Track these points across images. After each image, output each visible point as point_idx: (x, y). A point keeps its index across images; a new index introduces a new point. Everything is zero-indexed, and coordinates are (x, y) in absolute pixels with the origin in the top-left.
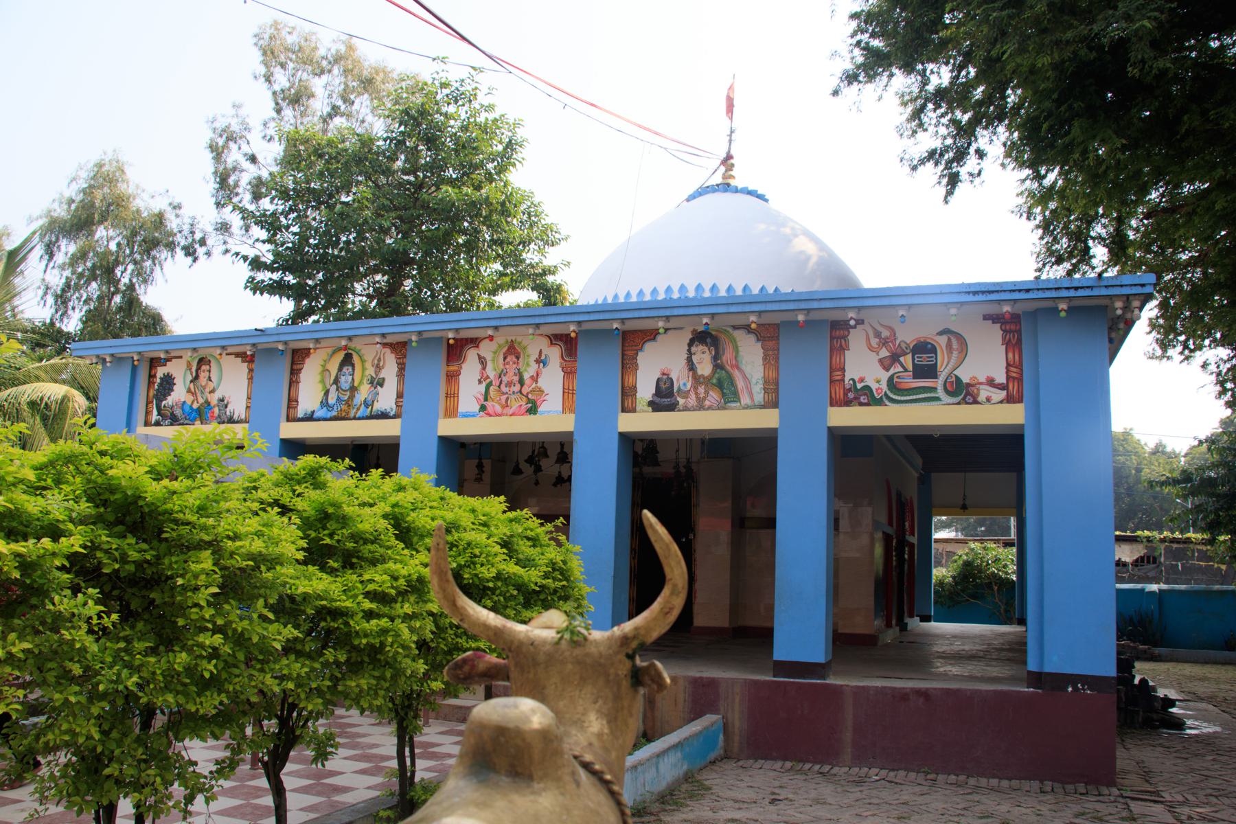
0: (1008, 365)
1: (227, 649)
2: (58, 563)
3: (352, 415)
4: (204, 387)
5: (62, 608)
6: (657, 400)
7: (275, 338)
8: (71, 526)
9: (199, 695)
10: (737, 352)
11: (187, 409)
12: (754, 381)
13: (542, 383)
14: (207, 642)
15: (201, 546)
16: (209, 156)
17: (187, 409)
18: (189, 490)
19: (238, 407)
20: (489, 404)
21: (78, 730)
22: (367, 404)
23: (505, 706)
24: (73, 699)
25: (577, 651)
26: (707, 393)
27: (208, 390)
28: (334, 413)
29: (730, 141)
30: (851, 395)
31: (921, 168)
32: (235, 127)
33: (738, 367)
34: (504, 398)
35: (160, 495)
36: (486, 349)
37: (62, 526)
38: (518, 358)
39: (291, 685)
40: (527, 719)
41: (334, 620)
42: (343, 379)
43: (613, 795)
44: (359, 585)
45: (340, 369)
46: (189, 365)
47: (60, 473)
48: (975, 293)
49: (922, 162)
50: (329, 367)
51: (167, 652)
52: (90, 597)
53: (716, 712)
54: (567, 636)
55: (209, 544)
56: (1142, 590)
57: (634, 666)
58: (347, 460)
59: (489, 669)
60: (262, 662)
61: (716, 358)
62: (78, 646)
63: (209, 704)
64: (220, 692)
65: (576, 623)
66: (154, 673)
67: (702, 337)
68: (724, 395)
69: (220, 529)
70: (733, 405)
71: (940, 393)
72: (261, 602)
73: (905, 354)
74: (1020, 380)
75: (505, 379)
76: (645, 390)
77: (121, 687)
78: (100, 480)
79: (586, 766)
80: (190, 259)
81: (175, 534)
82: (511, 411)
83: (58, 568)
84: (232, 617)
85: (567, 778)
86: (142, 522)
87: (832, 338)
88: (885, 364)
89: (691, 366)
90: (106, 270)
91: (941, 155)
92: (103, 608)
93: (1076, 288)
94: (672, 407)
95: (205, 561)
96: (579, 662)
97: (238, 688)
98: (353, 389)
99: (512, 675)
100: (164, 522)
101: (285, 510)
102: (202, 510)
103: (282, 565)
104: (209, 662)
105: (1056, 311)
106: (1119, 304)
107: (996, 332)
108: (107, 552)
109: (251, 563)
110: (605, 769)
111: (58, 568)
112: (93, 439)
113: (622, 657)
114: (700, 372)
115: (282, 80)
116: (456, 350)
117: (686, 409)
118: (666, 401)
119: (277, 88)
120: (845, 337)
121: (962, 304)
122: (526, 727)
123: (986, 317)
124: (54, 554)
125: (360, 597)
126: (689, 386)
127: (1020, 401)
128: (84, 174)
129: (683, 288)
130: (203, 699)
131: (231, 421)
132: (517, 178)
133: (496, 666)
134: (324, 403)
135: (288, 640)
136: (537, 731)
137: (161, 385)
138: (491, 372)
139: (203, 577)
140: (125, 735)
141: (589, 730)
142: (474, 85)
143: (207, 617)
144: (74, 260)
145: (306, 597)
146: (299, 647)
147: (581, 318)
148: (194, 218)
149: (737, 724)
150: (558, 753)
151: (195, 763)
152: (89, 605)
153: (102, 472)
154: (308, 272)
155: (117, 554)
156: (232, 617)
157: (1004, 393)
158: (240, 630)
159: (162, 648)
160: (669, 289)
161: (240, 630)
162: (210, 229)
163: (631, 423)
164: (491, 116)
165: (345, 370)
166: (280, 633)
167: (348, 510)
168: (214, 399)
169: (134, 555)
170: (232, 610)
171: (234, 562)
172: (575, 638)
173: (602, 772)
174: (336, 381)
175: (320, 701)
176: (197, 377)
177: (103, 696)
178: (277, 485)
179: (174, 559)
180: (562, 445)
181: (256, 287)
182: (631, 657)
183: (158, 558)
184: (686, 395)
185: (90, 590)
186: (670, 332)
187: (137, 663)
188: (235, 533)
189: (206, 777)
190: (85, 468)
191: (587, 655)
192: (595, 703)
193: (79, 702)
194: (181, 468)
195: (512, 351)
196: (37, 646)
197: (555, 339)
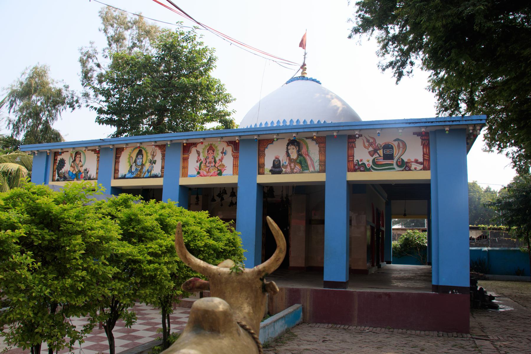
0: (424, 154)
1: (88, 277)
2: (14, 241)
3: (142, 176)
4: (78, 165)
5: (16, 260)
6: (274, 169)
7: (109, 143)
8: (20, 225)
9: (76, 297)
10: (308, 148)
11: (71, 174)
12: (315, 161)
13: (224, 162)
14: (80, 275)
15: (77, 233)
16: (25, 68)
17: (71, 174)
18: (72, 209)
19: (93, 173)
20: (201, 171)
21: (24, 313)
22: (148, 171)
23: (208, 301)
24: (21, 299)
25: (239, 277)
26: (295, 166)
27: (80, 166)
28: (134, 175)
29: (305, 58)
31: (387, 70)
32: (91, 52)
34: (207, 169)
35: (59, 211)
36: (200, 148)
37: (16, 225)
38: (214, 151)
39: (116, 293)
40: (218, 307)
41: (135, 264)
42: (138, 161)
43: (255, 339)
44: (145, 250)
45: (137, 156)
46: (71, 154)
47: (15, 202)
48: (410, 123)
49: (387, 67)
50: (132, 155)
51: (62, 279)
52: (29, 255)
53: (299, 303)
54: (234, 271)
55: (80, 232)
56: (481, 250)
57: (263, 283)
58: (140, 196)
59: (201, 285)
60: (103, 283)
61: (298, 151)
62: (23, 276)
63: (81, 301)
64: (85, 296)
65: (238, 265)
66: (57, 288)
67: (293, 142)
68: (302, 167)
69: (85, 226)
70: (306, 171)
71: (395, 166)
72: (103, 257)
73: (380, 149)
74: (429, 160)
75: (208, 161)
76: (268, 165)
77: (42, 294)
78: (32, 205)
79: (243, 327)
80: (71, 109)
81: (65, 228)
82: (211, 174)
83: (15, 243)
84: (91, 264)
85: (235, 332)
86: (51, 223)
87: (348, 143)
88: (371, 154)
89: (288, 155)
90: (35, 114)
91: (395, 64)
92: (34, 260)
93: (453, 121)
94: (280, 172)
95: (79, 239)
96: (240, 282)
97: (93, 294)
98: (143, 165)
99: (211, 288)
100: (61, 223)
101: (113, 217)
102: (77, 217)
103: (112, 241)
104: (81, 283)
105: (444, 131)
106: (471, 128)
107: (419, 140)
108: (36, 236)
109: (99, 240)
110: (251, 328)
111: (15, 243)
112: (29, 187)
113: (258, 279)
114: (292, 157)
115: (111, 32)
116: (187, 148)
117: (286, 173)
119: (109, 35)
120: (354, 142)
121: (404, 128)
122: (217, 310)
123: (414, 134)
124: (13, 237)
125: (146, 255)
126: (287, 163)
127: (429, 169)
129: (284, 121)
130: (78, 299)
131: (90, 179)
132: (213, 74)
133: (204, 284)
134: (130, 171)
135: (115, 273)
136: (221, 312)
137: (59, 163)
138: (202, 158)
139: (78, 246)
140: (44, 315)
141: (244, 311)
142: (194, 34)
143: (80, 263)
144: (21, 110)
145: (122, 255)
146: (119, 276)
147: (241, 134)
148: (73, 91)
149: (308, 308)
150: (230, 321)
151: (75, 327)
152: (28, 259)
153: (33, 201)
154: (122, 114)
155: (40, 237)
156: (91, 264)
157: (421, 167)
158: (94, 269)
159: (60, 277)
160: (278, 122)
161: (94, 269)
162: (80, 96)
163: (263, 179)
164: (201, 47)
165: (139, 157)
166: (111, 270)
167: (140, 217)
168: (82, 170)
169: (48, 237)
170: (91, 261)
171: (91, 240)
172: (238, 272)
173: (250, 329)
174: (135, 162)
175: (129, 299)
176: (75, 160)
177: (35, 298)
178: (110, 206)
179: (65, 239)
180: (233, 189)
181: (100, 121)
182: (262, 280)
183: (58, 238)
184: (286, 167)
185: (29, 252)
186: (279, 140)
187: (49, 284)
188: (92, 227)
189: (79, 333)
190: (26, 200)
191: (243, 279)
192: (247, 299)
193: (24, 301)
194: (68, 199)
195: (211, 148)
196: (5, 277)
197: (230, 143)
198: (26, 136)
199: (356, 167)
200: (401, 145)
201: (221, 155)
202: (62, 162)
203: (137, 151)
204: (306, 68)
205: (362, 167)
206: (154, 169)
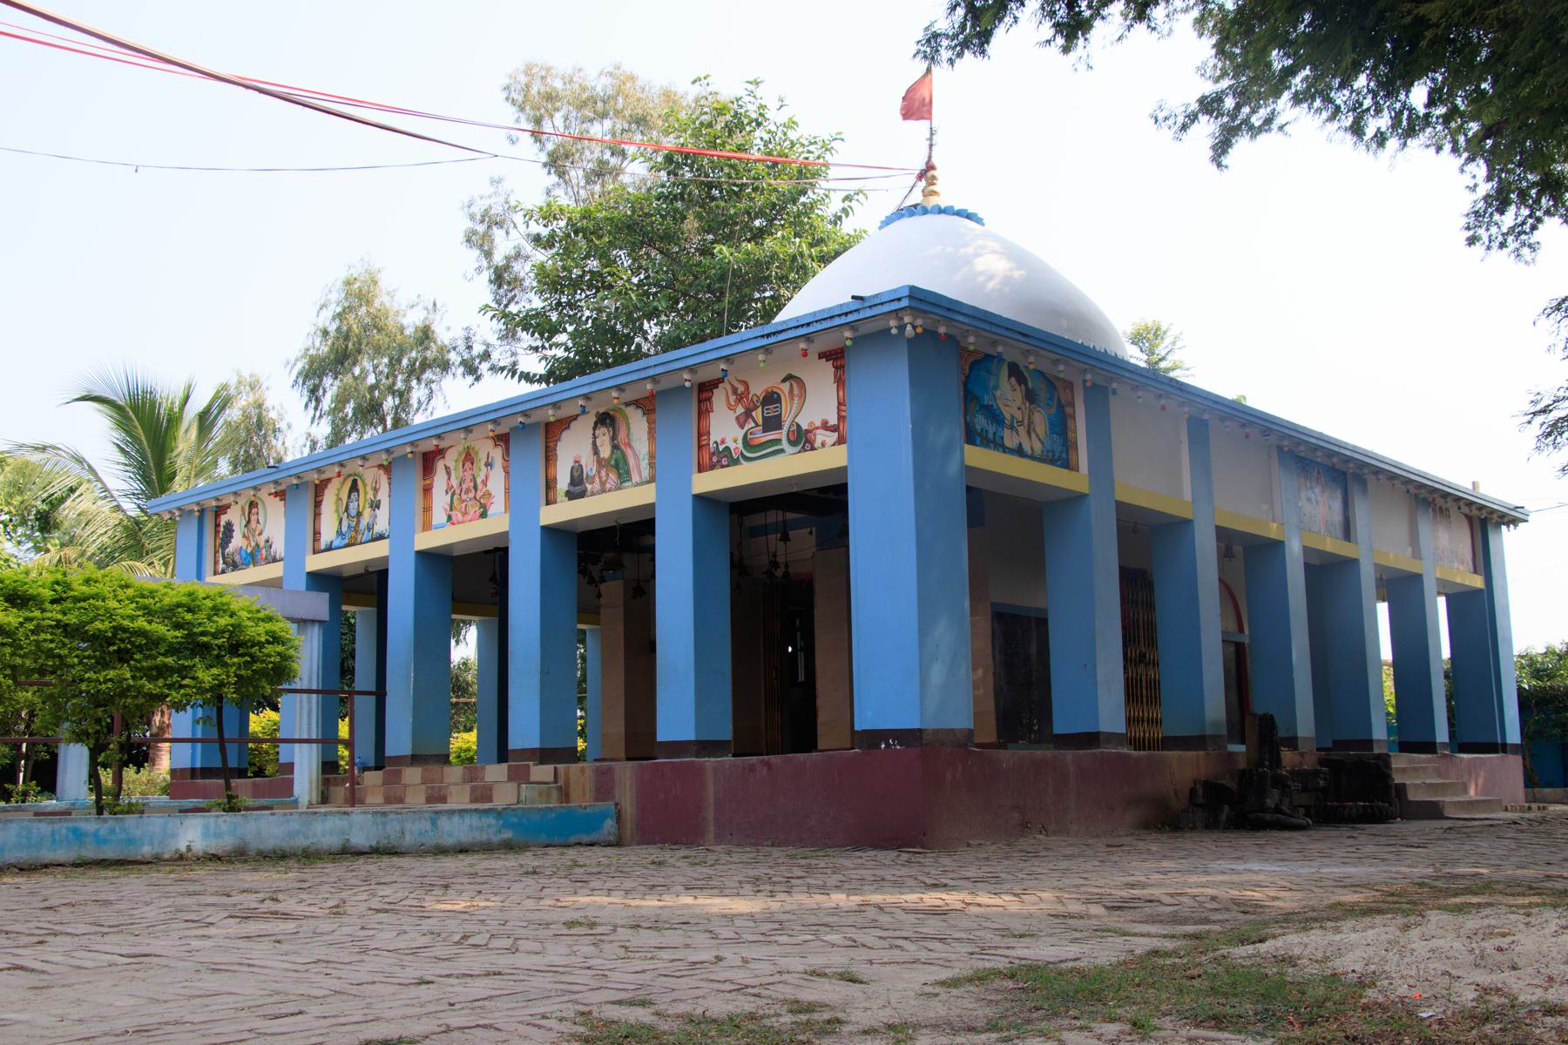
19: (279, 548)
20: (453, 513)
30: (715, 459)
32: (497, 210)
33: (629, 445)
36: (451, 459)
49: (1193, 118)
61: (613, 438)
67: (606, 420)
68: (620, 475)
71: (785, 445)
73: (756, 408)
76: (563, 482)
87: (700, 401)
93: (846, 314)
94: (582, 495)
98: (359, 514)
107: (828, 368)
116: (429, 461)
117: (593, 494)
118: (578, 489)
120: (709, 399)
121: (766, 349)
128: (334, 297)
131: (275, 560)
134: (340, 533)
162: (493, 339)
163: (553, 515)
176: (249, 522)
195: (469, 457)
199: (715, 459)
200: (796, 391)
201: (484, 469)
204: (934, 177)
206: (378, 520)
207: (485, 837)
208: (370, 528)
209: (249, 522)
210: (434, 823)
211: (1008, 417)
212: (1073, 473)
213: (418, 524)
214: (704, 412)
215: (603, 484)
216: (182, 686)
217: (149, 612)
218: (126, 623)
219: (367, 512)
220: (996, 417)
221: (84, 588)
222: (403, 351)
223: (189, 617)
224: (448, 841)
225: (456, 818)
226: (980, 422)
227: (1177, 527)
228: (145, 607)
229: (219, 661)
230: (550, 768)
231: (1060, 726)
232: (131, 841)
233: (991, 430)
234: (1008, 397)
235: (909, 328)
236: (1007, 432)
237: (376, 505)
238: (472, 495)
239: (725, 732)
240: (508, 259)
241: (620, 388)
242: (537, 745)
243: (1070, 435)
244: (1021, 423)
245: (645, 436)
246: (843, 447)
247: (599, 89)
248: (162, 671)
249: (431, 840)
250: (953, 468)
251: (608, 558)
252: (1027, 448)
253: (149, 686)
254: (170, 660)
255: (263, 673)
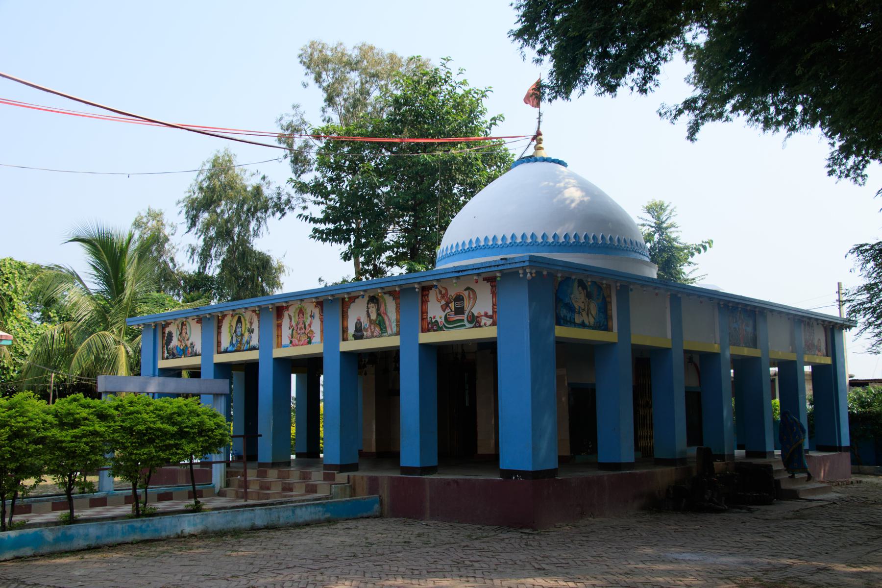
19: (198, 348)
29: (539, 122)
33: (386, 314)
36: (292, 311)
48: (459, 272)
61: (378, 310)
67: (373, 299)
68: (381, 329)
71: (466, 322)
76: (351, 330)
87: (422, 296)
89: (369, 316)
98: (242, 335)
107: (487, 286)
117: (367, 338)
120: (427, 295)
121: (458, 278)
123: (484, 279)
131: (196, 355)
134: (231, 343)
154: (351, 219)
157: (491, 320)
160: (486, 239)
174: (235, 332)
176: (181, 333)
184: (366, 330)
195: (301, 312)
198: (224, 265)
202: (170, 334)
203: (236, 318)
205: (432, 326)
207: (317, 517)
208: (248, 342)
209: (181, 333)
210: (293, 512)
211: (577, 307)
212: (610, 333)
213: (275, 344)
214: (424, 302)
215: (372, 333)
216: (177, 454)
217: (161, 418)
218: (152, 425)
219: (246, 334)
220: (571, 308)
221: (132, 408)
222: (244, 202)
223: (179, 419)
224: (301, 520)
225: (304, 509)
226: (564, 312)
227: (661, 353)
228: (159, 415)
229: (193, 440)
230: (345, 475)
231: (603, 457)
232: (156, 530)
233: (569, 315)
234: (578, 298)
235: (529, 275)
236: (577, 316)
237: (251, 331)
238: (303, 331)
239: (434, 462)
240: (300, 148)
241: (382, 288)
242: (337, 462)
243: (609, 312)
244: (583, 310)
245: (394, 310)
246: (495, 328)
247: (354, 56)
248: (168, 447)
249: (292, 520)
250: (551, 339)
251: (375, 371)
252: (587, 322)
253: (163, 455)
254: (172, 442)
255: (213, 444)
